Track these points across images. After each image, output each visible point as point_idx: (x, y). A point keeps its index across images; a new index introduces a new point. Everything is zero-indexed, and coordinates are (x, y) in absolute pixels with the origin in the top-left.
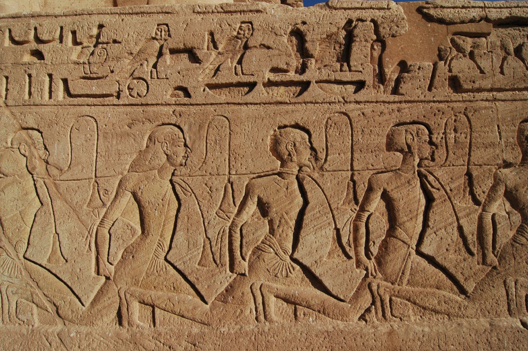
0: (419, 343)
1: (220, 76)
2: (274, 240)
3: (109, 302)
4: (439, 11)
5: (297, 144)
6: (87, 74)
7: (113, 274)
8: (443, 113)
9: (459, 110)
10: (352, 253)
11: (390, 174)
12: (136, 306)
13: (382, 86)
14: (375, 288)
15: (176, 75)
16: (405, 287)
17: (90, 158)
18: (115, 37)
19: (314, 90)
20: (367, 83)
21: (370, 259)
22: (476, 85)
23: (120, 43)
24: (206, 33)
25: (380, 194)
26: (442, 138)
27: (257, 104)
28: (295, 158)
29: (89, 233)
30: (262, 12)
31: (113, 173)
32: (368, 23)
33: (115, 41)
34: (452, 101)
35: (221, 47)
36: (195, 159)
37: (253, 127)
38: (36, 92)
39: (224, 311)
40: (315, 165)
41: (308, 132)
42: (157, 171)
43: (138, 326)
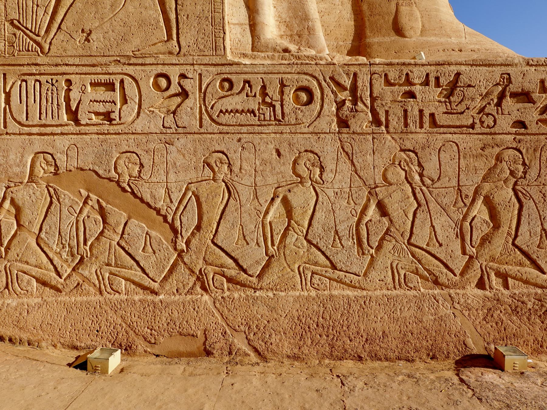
3: (475, 273)
15: (515, 112)
17: (454, 172)
18: (469, 83)
29: (456, 225)
31: (471, 183)
33: (469, 86)
36: (533, 173)
38: (412, 123)
43: (496, 289)
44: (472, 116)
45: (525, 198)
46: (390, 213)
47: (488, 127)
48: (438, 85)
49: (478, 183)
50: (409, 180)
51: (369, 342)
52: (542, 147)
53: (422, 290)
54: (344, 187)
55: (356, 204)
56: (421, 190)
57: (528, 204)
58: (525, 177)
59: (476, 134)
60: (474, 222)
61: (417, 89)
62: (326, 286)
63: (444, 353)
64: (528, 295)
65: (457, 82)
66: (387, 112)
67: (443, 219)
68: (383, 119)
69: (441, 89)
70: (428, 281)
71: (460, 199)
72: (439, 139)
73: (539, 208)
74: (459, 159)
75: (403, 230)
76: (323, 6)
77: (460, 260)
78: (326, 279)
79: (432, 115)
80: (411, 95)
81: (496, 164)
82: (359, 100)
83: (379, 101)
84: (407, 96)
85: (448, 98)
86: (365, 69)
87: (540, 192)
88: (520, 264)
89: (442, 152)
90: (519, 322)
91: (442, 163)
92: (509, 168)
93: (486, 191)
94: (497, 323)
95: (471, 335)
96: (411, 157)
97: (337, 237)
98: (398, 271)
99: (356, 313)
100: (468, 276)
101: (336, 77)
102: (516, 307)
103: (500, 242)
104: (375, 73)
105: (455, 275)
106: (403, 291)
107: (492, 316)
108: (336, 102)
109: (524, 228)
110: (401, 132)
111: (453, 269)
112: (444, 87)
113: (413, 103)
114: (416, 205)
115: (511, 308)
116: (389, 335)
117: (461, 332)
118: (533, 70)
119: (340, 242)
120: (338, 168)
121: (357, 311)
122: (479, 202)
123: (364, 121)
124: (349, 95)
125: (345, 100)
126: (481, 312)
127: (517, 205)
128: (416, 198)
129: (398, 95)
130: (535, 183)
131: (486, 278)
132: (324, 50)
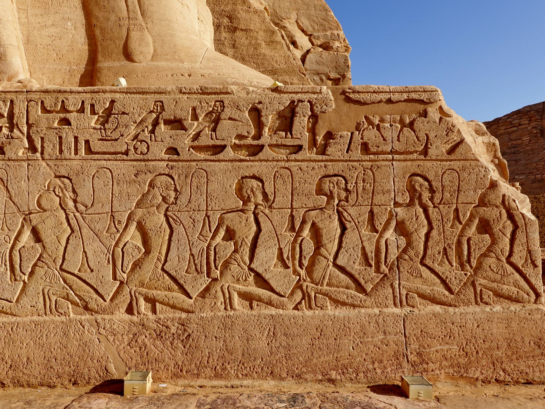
0: (331, 322)
1: (200, 140)
2: (238, 256)
3: (124, 298)
4: (357, 95)
5: (254, 189)
7: (126, 280)
8: (356, 169)
9: (366, 167)
10: (290, 265)
11: (318, 211)
13: (315, 149)
14: (304, 288)
15: (168, 139)
16: (325, 287)
17: (107, 198)
20: (304, 147)
21: (302, 269)
22: (380, 149)
23: (128, 114)
24: (191, 109)
25: (310, 224)
26: (354, 186)
27: (226, 161)
28: (252, 199)
30: (230, 94)
31: (124, 209)
32: (306, 103)
33: (124, 113)
34: (362, 161)
35: (200, 119)
36: (184, 199)
37: (224, 176)
38: (66, 150)
39: (203, 303)
40: (266, 204)
41: (261, 181)
42: (155, 208)
43: (144, 314)
44: (126, 143)
45: (176, 224)
46: (43, 239)
47: (142, 153)
48: (93, 112)
49: (131, 209)
50: (63, 206)
51: (13, 368)
52: (193, 173)
53: (72, 315)
56: (74, 216)
57: (179, 230)
58: (176, 203)
59: (131, 160)
60: (125, 247)
61: (72, 117)
63: (85, 379)
64: (173, 320)
65: (112, 110)
66: (42, 139)
69: (96, 117)
70: (79, 307)
71: (113, 225)
72: (92, 166)
73: (188, 234)
75: (55, 256)
76: (54, 30)
79: (87, 142)
80: (67, 122)
81: (149, 190)
82: (15, 127)
83: (34, 128)
84: (64, 122)
85: (104, 125)
86: (21, 97)
87: (190, 217)
88: (169, 288)
90: (162, 346)
91: (95, 189)
92: (161, 194)
94: (140, 348)
95: (113, 360)
96: (65, 183)
98: (49, 297)
100: (117, 302)
102: (161, 332)
103: (150, 268)
104: (31, 101)
105: (105, 301)
106: (52, 317)
107: (136, 341)
109: (173, 253)
110: (56, 159)
111: (103, 294)
112: (100, 114)
113: (67, 130)
114: (69, 231)
115: (156, 333)
116: (33, 362)
117: (104, 358)
118: (185, 98)
121: (3, 337)
122: (133, 228)
124: (7, 122)
126: (126, 337)
127: (168, 231)
128: (69, 224)
129: (54, 122)
130: (186, 209)
132: (17, 76)
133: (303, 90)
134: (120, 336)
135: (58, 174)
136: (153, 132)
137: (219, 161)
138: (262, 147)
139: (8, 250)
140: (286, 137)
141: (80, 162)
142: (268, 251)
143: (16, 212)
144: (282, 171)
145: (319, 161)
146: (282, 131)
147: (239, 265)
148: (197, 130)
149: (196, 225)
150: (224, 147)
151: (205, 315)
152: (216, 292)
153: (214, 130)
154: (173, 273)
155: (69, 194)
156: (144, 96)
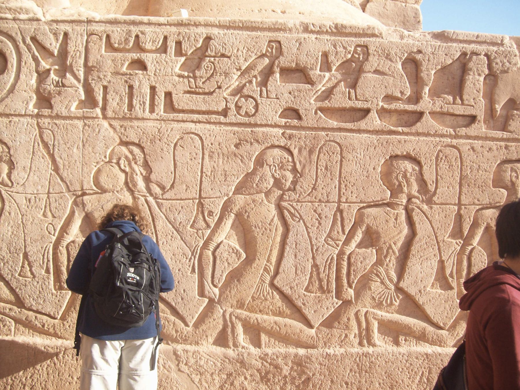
2: (381, 270)
5: (408, 174)
6: (192, 88)
7: (217, 297)
10: (454, 284)
12: (240, 329)
15: (286, 95)
17: (195, 177)
19: (428, 122)
20: (478, 118)
23: (229, 57)
24: (320, 54)
25: (483, 228)
28: (405, 189)
29: (192, 254)
31: (218, 194)
32: (482, 57)
33: (223, 55)
35: (334, 68)
36: (306, 184)
38: (138, 105)
40: (424, 198)
41: (418, 163)
42: (263, 194)
43: (243, 347)
44: (225, 98)
47: (247, 114)
48: (179, 52)
49: (228, 195)
50: (131, 186)
52: (321, 148)
54: (40, 192)
55: (55, 217)
56: (146, 201)
57: (298, 228)
58: (294, 190)
60: (218, 250)
61: (149, 58)
62: (10, 330)
64: (285, 357)
66: (105, 88)
67: (175, 245)
68: (100, 98)
69: (183, 59)
71: (200, 216)
73: (311, 234)
74: (203, 158)
77: (195, 303)
78: (10, 320)
79: (168, 95)
80: (142, 65)
81: (255, 169)
83: (95, 74)
84: (136, 66)
86: (80, 29)
87: (315, 211)
89: (178, 147)
91: (178, 164)
92: (273, 176)
93: (238, 207)
96: (135, 153)
97: (26, 262)
99: (45, 369)
101: (40, 38)
102: (267, 373)
103: (255, 280)
105: (187, 325)
107: (232, 384)
108: (37, 72)
109: (288, 262)
111: (185, 316)
113: (141, 76)
115: (260, 374)
118: (313, 39)
119: (31, 270)
120: (33, 165)
123: (72, 100)
125: (49, 71)
127: (281, 230)
129: (122, 65)
130: (309, 198)
131: (229, 330)
133: (479, 39)
134: (208, 376)
135: (124, 139)
136: (264, 83)
137: (359, 131)
138: (421, 114)
139: (52, 245)
140: (454, 103)
141: (157, 124)
142: (425, 264)
143: (64, 191)
144: (448, 150)
145: (498, 140)
146: (448, 94)
147: (382, 283)
148: (328, 85)
149: (323, 222)
150: (367, 111)
151: (331, 351)
152: (349, 319)
153: (354, 86)
154: (287, 290)
155: (139, 169)
156: (254, 33)
